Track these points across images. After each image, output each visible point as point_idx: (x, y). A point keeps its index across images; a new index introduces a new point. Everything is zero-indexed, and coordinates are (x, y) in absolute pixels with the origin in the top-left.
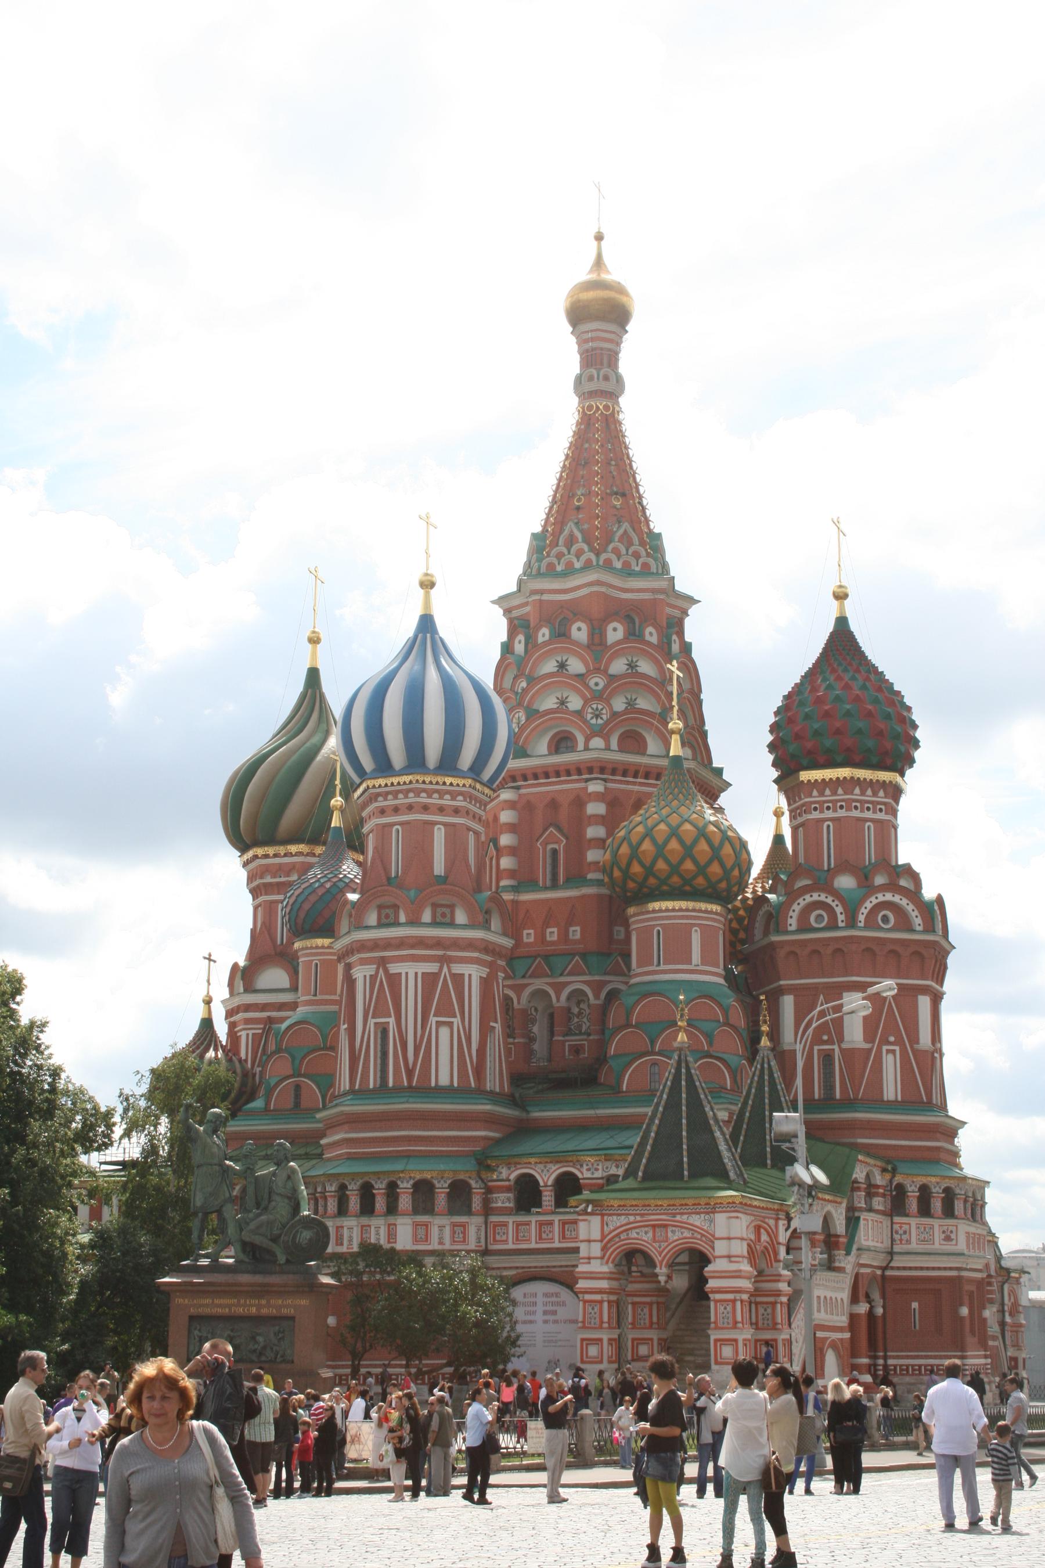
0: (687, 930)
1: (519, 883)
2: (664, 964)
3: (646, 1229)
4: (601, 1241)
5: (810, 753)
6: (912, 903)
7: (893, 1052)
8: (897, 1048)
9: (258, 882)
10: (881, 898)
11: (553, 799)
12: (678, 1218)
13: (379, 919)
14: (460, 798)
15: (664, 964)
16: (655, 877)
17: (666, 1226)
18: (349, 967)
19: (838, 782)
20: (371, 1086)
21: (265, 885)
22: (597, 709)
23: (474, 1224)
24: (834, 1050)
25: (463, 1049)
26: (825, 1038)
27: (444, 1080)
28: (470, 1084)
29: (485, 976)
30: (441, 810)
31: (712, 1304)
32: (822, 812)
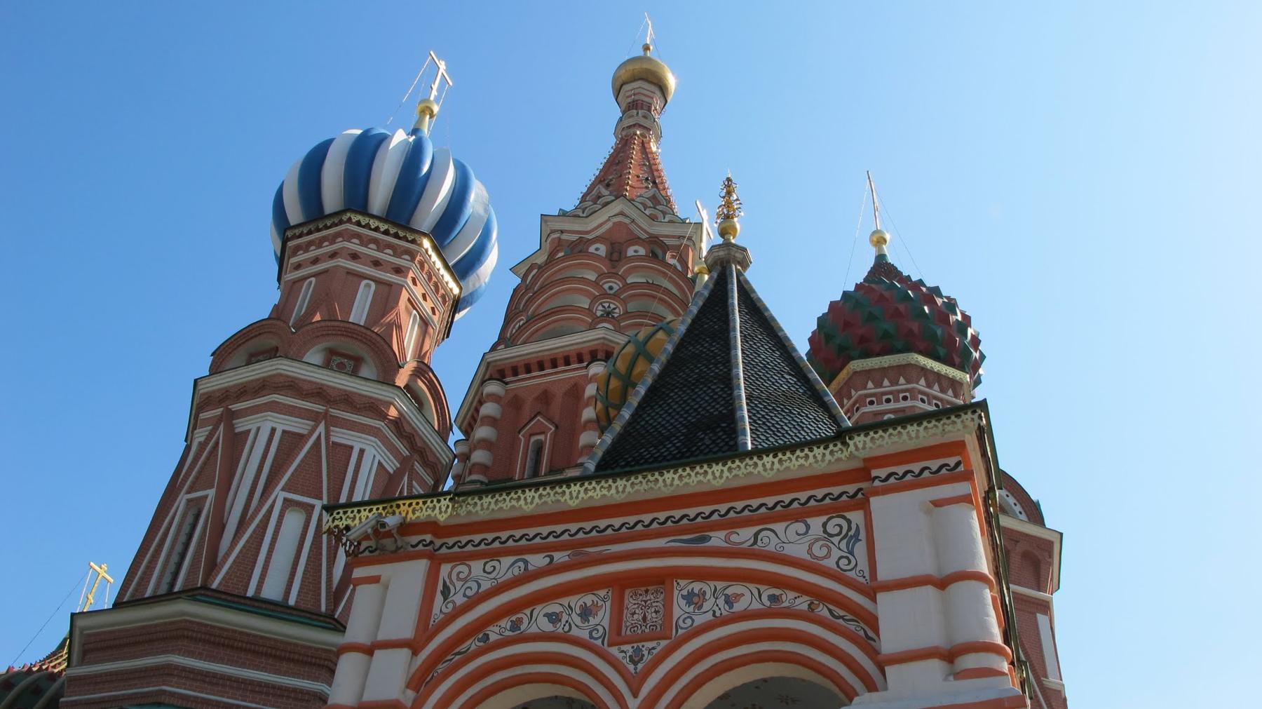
1: (489, 482)
3: (588, 599)
4: (414, 646)
5: (863, 340)
6: (1012, 494)
11: (546, 390)
12: (717, 539)
17: (661, 580)
19: (903, 370)
20: (147, 595)
22: (609, 307)
25: (321, 548)
27: (272, 591)
28: (320, 606)
29: (391, 471)
30: (377, 263)
32: (880, 403)
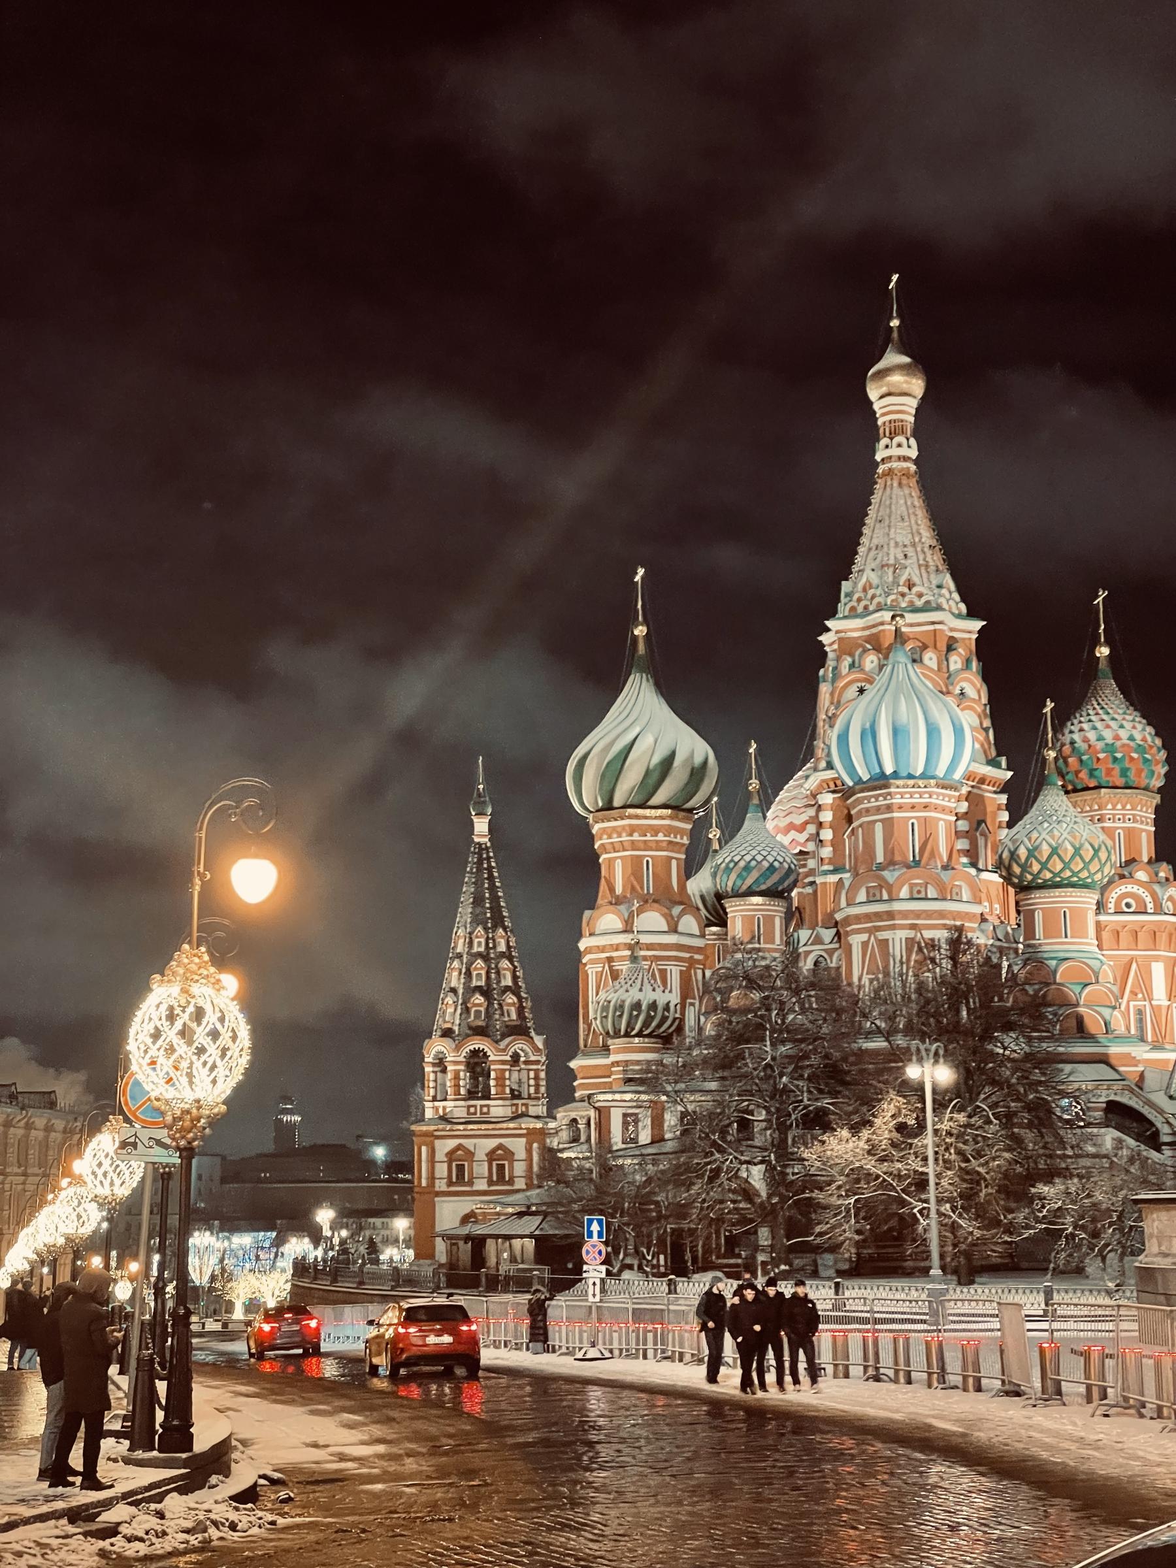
9: (625, 838)
10: (1171, 893)
14: (953, 800)
16: (1072, 871)
21: (633, 842)
26: (1140, 996)
30: (943, 810)
32: (1114, 822)
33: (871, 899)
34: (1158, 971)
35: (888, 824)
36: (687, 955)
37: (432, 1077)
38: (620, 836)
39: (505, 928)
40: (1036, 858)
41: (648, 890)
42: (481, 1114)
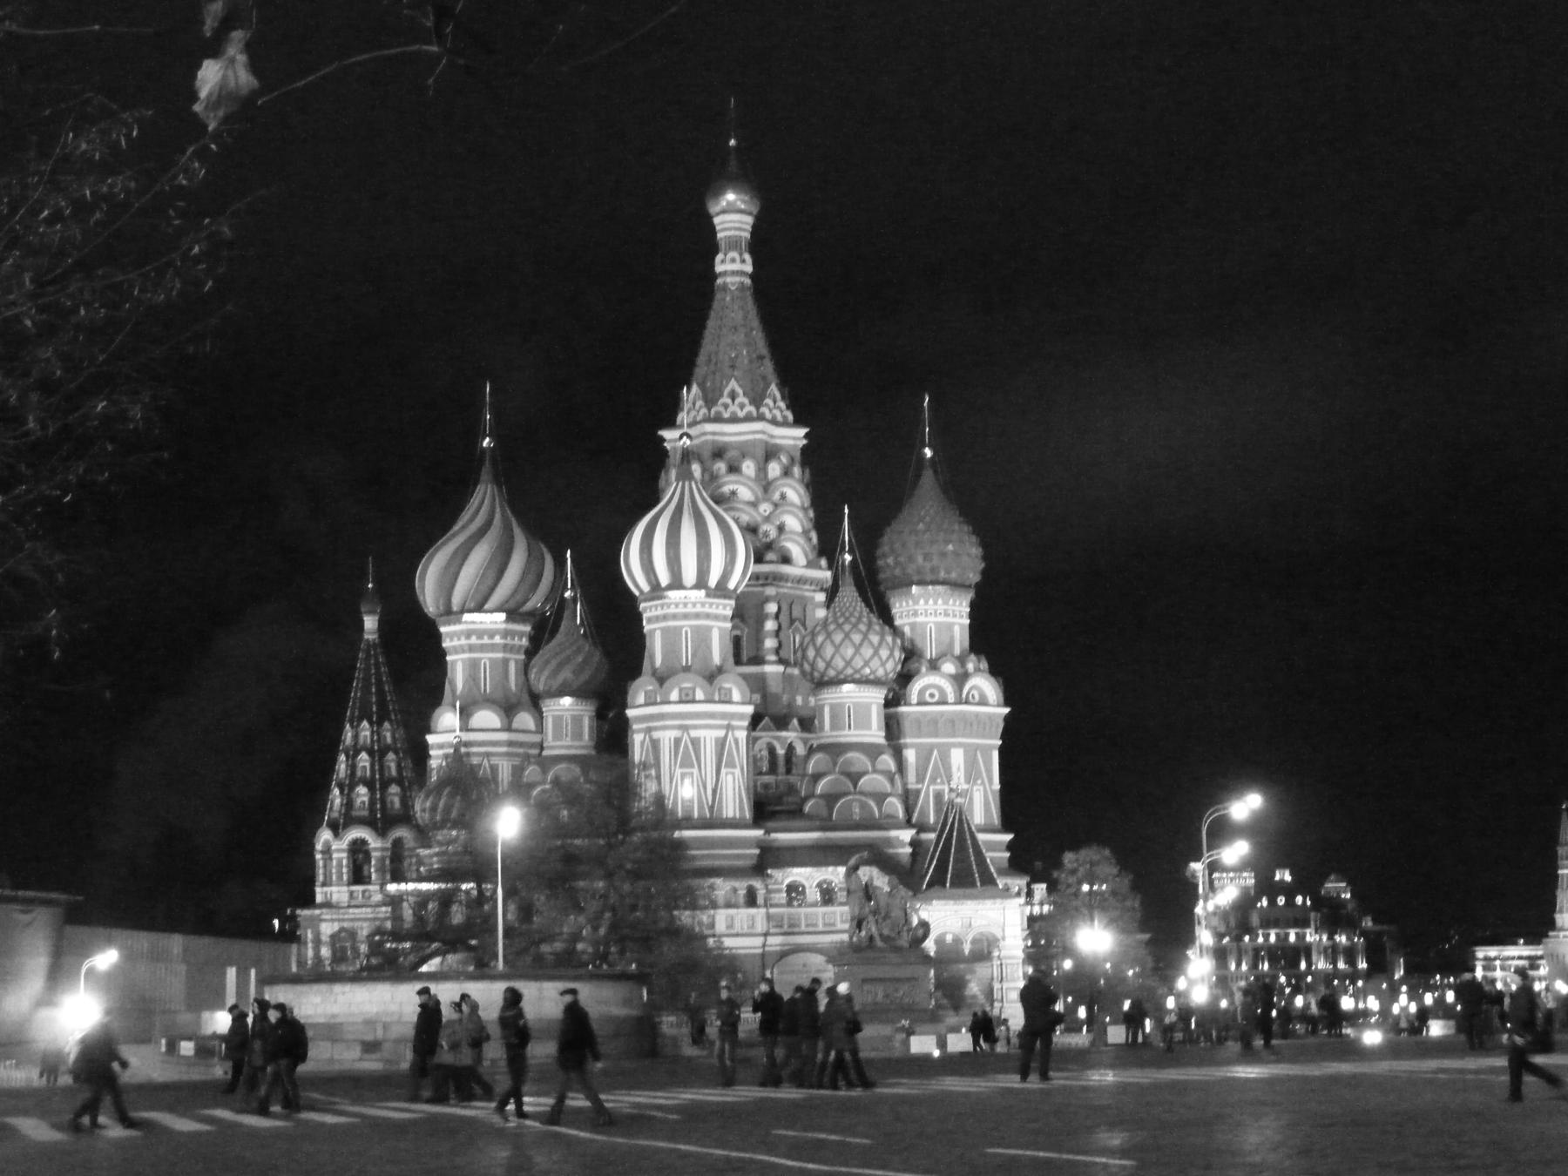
0: (868, 707)
2: (854, 729)
7: (979, 790)
8: (981, 788)
9: (463, 641)
13: (680, 696)
14: (728, 608)
15: (854, 729)
16: (853, 669)
17: (971, 918)
18: (649, 730)
23: (759, 913)
24: (944, 790)
26: (939, 781)
27: (731, 815)
30: (716, 617)
31: (1004, 967)
32: (926, 616)
33: (648, 701)
34: (957, 758)
35: (665, 631)
36: (521, 750)
37: (321, 863)
38: (459, 639)
39: (390, 721)
40: (821, 657)
41: (485, 690)
42: (363, 896)
